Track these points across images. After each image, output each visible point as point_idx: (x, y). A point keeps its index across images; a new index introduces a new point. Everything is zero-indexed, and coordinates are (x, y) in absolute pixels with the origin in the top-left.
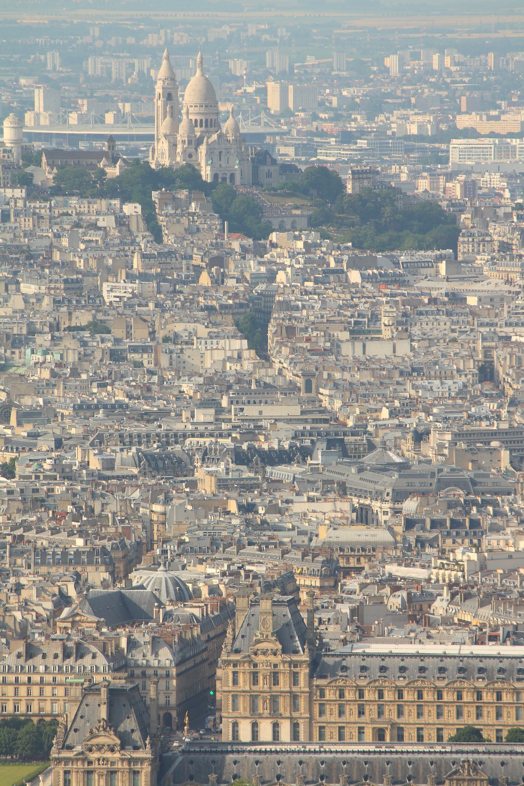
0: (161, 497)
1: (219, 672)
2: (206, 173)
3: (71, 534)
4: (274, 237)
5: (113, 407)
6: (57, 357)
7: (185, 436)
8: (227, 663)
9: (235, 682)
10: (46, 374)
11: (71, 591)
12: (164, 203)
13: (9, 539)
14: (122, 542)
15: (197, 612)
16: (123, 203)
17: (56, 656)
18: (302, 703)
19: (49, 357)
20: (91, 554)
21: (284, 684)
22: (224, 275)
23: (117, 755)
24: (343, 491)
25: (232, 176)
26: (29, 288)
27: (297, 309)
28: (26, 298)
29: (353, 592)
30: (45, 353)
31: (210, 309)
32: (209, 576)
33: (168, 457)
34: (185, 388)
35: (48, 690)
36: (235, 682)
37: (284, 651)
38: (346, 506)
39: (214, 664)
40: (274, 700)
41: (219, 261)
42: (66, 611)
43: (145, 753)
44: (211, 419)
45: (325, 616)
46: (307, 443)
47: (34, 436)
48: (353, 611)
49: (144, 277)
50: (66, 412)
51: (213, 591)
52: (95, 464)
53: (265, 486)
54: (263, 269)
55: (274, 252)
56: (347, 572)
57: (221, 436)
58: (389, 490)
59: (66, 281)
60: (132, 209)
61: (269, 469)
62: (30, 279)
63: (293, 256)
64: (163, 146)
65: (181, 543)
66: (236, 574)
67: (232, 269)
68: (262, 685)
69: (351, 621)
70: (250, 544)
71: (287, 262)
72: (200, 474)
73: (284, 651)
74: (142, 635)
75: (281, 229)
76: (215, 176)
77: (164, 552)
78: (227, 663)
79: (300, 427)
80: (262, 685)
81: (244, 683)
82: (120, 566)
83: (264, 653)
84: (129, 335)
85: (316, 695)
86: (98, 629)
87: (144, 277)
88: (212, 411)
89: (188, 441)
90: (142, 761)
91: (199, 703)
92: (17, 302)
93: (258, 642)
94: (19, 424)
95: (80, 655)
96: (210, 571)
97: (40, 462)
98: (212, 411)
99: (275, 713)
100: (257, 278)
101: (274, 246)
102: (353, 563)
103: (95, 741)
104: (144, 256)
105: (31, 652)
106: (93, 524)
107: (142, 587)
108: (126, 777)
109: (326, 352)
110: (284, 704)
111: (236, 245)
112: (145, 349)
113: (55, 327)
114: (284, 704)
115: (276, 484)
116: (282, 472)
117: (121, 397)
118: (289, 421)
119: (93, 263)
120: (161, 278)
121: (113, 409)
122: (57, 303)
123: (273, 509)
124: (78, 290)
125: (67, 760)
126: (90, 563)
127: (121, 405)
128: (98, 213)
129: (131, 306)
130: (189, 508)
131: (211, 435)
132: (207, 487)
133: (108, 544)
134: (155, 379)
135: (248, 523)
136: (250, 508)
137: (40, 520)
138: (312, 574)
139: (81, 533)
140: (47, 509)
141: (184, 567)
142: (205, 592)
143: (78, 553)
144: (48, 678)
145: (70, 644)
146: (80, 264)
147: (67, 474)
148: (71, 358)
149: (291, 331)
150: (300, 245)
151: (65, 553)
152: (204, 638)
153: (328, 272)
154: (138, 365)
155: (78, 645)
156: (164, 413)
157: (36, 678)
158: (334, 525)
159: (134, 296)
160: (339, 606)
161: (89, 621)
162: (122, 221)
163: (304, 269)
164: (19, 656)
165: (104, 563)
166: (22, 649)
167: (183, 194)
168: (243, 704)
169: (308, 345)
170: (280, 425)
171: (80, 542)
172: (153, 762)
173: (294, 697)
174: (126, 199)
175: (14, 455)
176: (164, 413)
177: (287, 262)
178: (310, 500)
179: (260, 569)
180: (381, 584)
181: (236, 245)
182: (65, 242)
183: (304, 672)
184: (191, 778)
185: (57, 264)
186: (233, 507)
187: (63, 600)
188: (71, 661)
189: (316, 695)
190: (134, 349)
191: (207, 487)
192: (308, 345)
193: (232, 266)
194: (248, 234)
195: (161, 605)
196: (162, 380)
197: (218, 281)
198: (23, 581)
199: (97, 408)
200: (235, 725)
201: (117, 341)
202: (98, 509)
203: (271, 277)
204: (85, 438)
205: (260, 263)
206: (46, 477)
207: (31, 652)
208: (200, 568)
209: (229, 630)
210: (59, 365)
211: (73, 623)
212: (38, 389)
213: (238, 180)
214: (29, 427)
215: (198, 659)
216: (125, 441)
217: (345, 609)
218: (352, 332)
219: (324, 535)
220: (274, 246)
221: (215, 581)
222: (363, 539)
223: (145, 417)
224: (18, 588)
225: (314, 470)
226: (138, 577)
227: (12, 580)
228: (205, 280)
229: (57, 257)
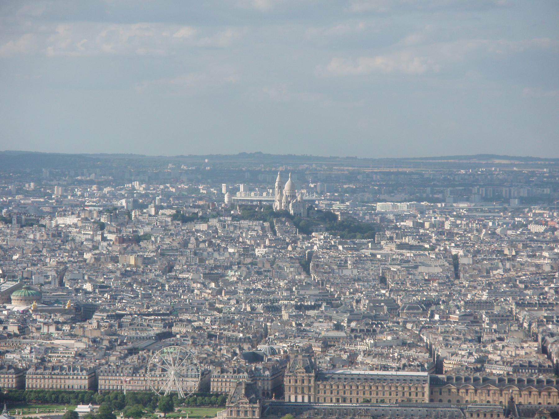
0: (270, 321)
1: (285, 379)
2: (292, 212)
3: (239, 332)
4: (313, 234)
5: (257, 290)
6: (239, 273)
7: (279, 300)
8: (287, 376)
9: (290, 382)
10: (235, 279)
11: (238, 351)
12: (277, 222)
13: (218, 334)
14: (256, 335)
15: (278, 359)
16: (264, 222)
17: (231, 373)
18: (312, 390)
19: (236, 273)
20: (245, 339)
21: (306, 383)
22: (296, 247)
23: (248, 406)
24: (331, 319)
25: (300, 214)
26: (231, 250)
27: (320, 258)
28: (230, 253)
29: (331, 353)
30: (235, 272)
31: (291, 258)
32: (283, 347)
33: (273, 307)
34: (281, 284)
35: (228, 384)
36: (290, 382)
37: (306, 372)
38: (332, 324)
39: (283, 376)
40: (303, 388)
41: (295, 242)
42: (235, 358)
43: (257, 405)
44: (289, 295)
45: (321, 361)
46: (320, 303)
47: (229, 299)
48: (330, 359)
49: (269, 247)
50: (241, 292)
51: (285, 352)
52: (249, 309)
53: (305, 317)
54: (309, 245)
55: (314, 239)
56: (330, 346)
57: (291, 300)
58: (346, 319)
59: (243, 248)
60: (266, 224)
61: (307, 312)
62: (232, 247)
63: (320, 240)
64: (277, 204)
65: (275, 336)
66: (293, 346)
67: (299, 245)
68: (299, 383)
69: (329, 362)
70: (299, 336)
71: (318, 242)
72: (283, 313)
73: (306, 372)
74: (260, 366)
75: (316, 231)
76: (295, 214)
77: (269, 339)
78: (287, 376)
79: (318, 298)
80: (299, 383)
81: (292, 383)
82: (255, 343)
83: (300, 373)
84: (263, 266)
85: (316, 387)
86: (245, 364)
87: (269, 247)
88: (289, 292)
89: (280, 302)
90: (256, 408)
91: (278, 389)
92: (227, 255)
93: (297, 369)
94: (225, 295)
95: (239, 373)
96: (284, 345)
97: (230, 308)
98: (289, 292)
99: (303, 393)
100: (307, 248)
101: (314, 237)
102: (332, 343)
103: (241, 401)
104: (269, 240)
105: (223, 371)
106: (247, 329)
107: (260, 350)
108: (251, 413)
109: (330, 273)
110: (306, 391)
111: (301, 237)
112: (268, 271)
113: (239, 263)
114: (306, 391)
115: (309, 317)
116: (311, 313)
117: (260, 287)
118: (315, 295)
119: (253, 242)
120: (275, 247)
121: (256, 291)
122: (240, 255)
123: (307, 325)
124: (247, 251)
125: (231, 407)
126: (245, 342)
127: (259, 289)
128: (256, 225)
129: (265, 257)
130: (279, 324)
131: (288, 300)
132: (285, 317)
133: (251, 336)
134: (272, 281)
135: (298, 329)
136: (300, 325)
137: (229, 327)
138: (319, 347)
139: (242, 332)
140: (232, 324)
141: (276, 344)
142: (282, 353)
143: (241, 339)
144: (228, 380)
145: (236, 369)
146: (249, 242)
147: (239, 312)
148: (244, 274)
149: (317, 266)
150: (322, 237)
151: (236, 339)
152: (281, 367)
153: (331, 246)
154: (266, 276)
155: (238, 369)
156: (273, 292)
157: (224, 380)
158: (328, 330)
159: (266, 253)
160: (326, 358)
161: (243, 362)
162: (263, 228)
163: (323, 245)
164: (218, 372)
165: (249, 342)
166: (219, 370)
167: (284, 219)
168: (292, 390)
169: (323, 270)
170: (311, 297)
171: (241, 335)
172: (259, 408)
173: (309, 388)
174: (265, 221)
175: (223, 306)
176: (273, 292)
177: (318, 242)
178: (320, 322)
179: (301, 345)
180: (341, 350)
181: (301, 237)
182: (244, 235)
183: (313, 380)
184: (272, 413)
185: (241, 242)
186: (294, 324)
187: (235, 354)
188: (236, 374)
189: (316, 387)
190: (265, 271)
191: (285, 317)
192: (323, 270)
193: (299, 243)
194: (304, 233)
195: (266, 356)
196: (274, 281)
197: (294, 248)
198: (222, 347)
199: (251, 290)
200: (290, 397)
201: (260, 268)
202: (249, 324)
203: (312, 247)
204: (246, 300)
205: (309, 243)
206: (232, 313)
207: (223, 371)
208: (281, 344)
209: (288, 365)
210: (240, 276)
211: (237, 362)
212: (232, 283)
213: (302, 215)
214: (228, 297)
215: (278, 375)
216: (259, 301)
217: (328, 358)
218: (338, 266)
219: (323, 334)
220: (314, 237)
221: (286, 349)
222: (336, 335)
223: (268, 294)
224: (221, 349)
225: (322, 312)
226: (259, 347)
227: (219, 347)
228: (290, 248)
229: (241, 240)
